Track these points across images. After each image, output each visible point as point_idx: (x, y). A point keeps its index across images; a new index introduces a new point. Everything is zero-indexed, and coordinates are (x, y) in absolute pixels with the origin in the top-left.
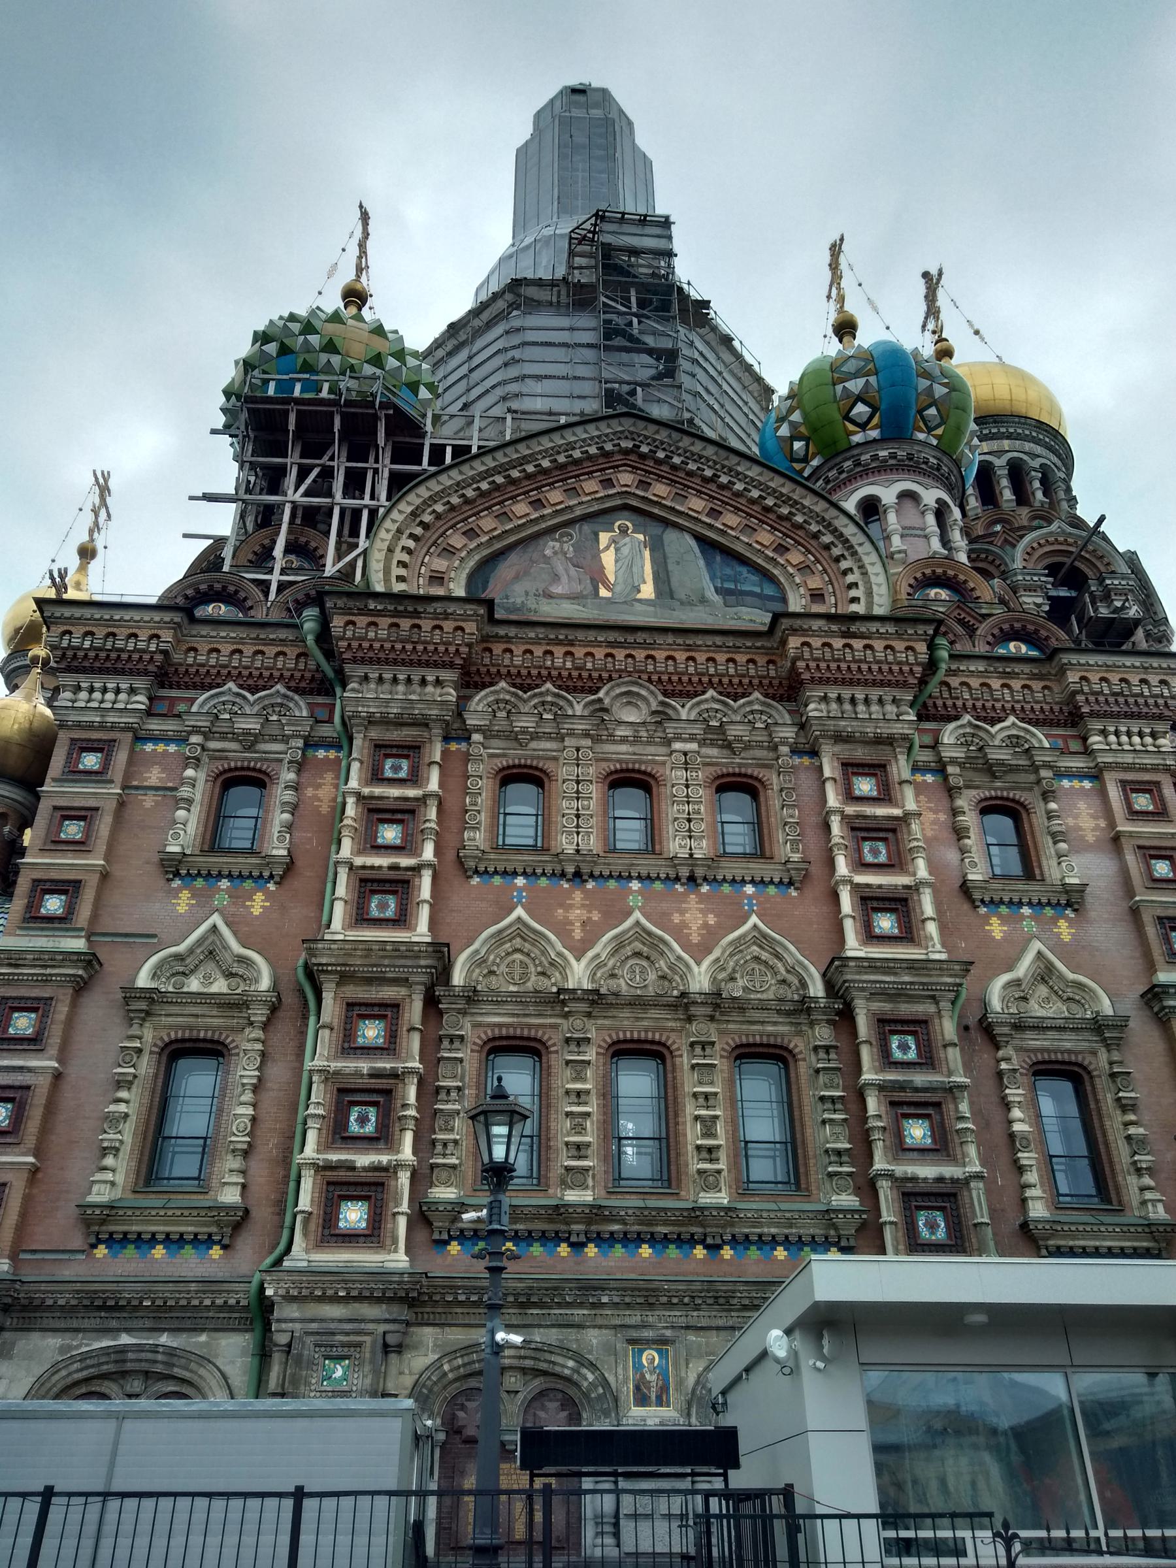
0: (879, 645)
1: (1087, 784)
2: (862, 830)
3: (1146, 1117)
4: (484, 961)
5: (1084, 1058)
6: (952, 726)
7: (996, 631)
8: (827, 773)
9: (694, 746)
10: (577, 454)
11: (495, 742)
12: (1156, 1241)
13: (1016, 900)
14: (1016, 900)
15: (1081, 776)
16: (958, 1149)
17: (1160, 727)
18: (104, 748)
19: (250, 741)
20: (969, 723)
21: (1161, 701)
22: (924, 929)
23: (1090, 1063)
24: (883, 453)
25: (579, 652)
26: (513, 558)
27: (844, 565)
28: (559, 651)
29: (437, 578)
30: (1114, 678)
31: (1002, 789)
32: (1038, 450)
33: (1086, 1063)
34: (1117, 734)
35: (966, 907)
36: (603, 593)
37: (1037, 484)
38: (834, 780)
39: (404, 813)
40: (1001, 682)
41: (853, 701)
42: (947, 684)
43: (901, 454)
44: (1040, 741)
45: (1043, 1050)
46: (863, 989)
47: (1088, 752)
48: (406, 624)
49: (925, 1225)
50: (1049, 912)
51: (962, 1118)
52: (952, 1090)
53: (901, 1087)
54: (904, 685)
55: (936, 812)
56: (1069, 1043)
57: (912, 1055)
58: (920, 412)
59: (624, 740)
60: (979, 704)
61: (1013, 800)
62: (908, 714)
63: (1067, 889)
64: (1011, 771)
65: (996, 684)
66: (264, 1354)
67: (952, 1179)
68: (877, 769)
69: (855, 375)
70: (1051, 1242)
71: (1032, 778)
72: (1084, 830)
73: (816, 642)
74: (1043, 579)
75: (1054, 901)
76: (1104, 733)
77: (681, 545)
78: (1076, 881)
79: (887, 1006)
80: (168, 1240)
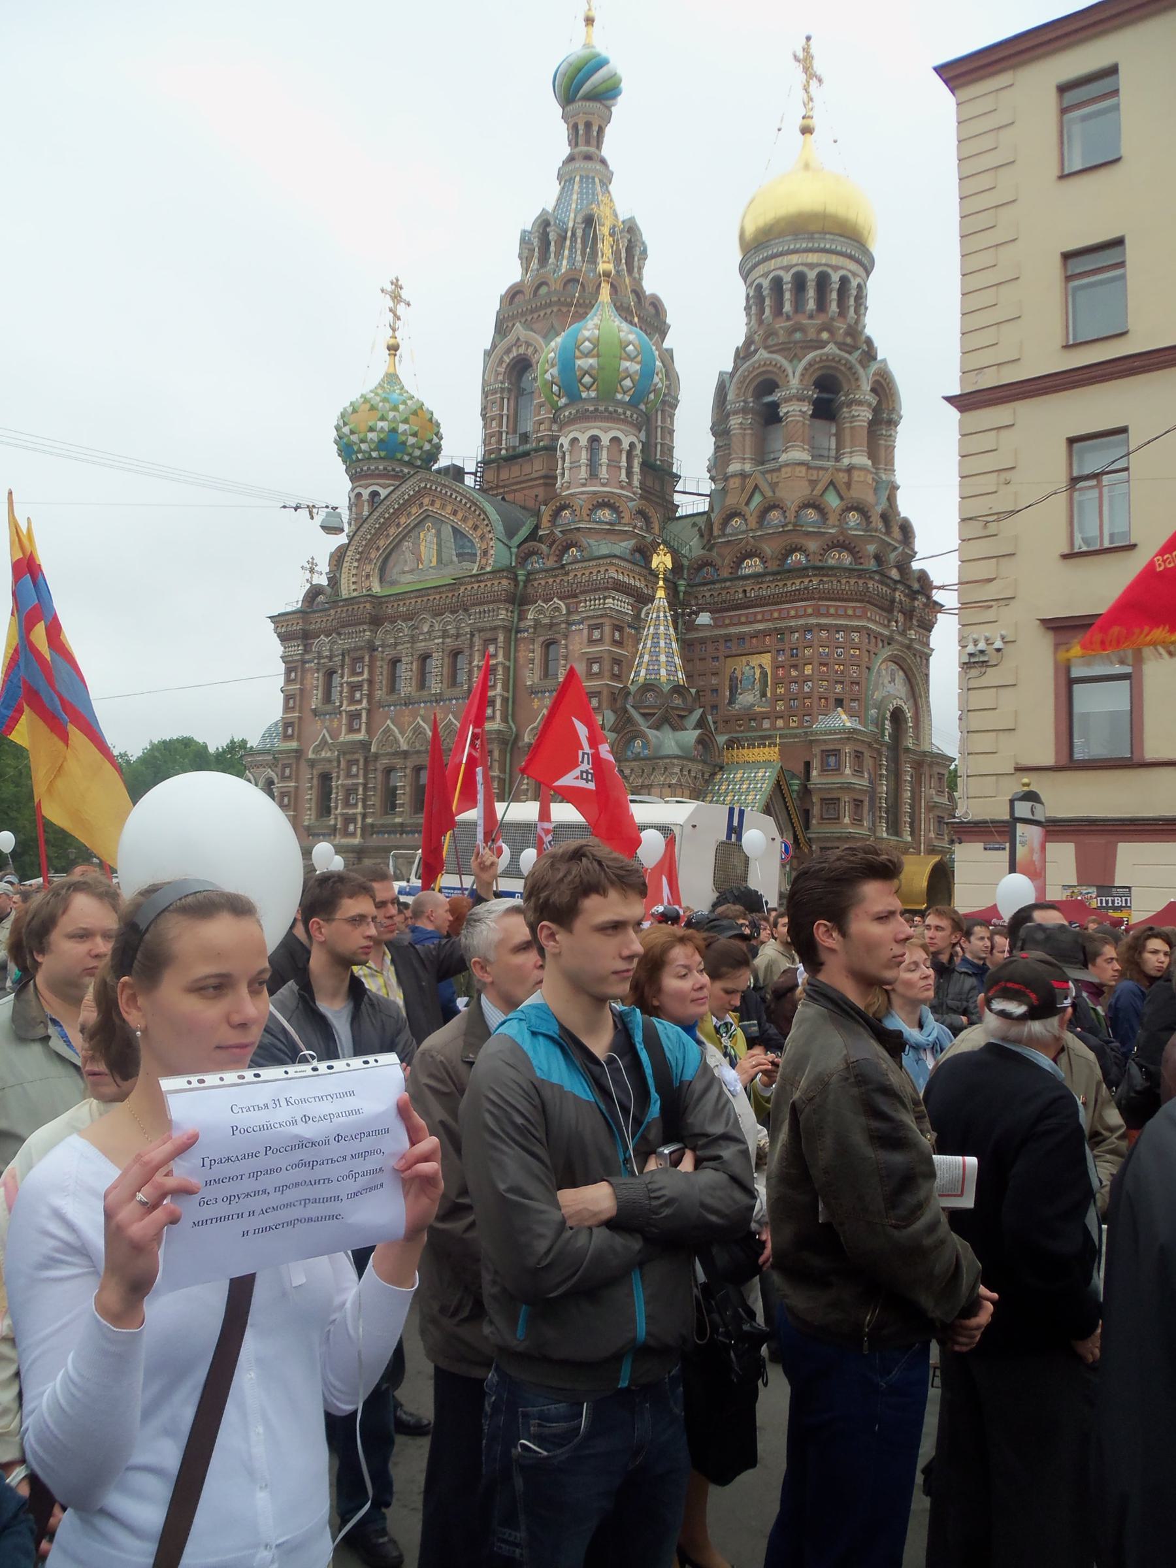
1: (581, 627)
4: (381, 741)
7: (560, 548)
9: (440, 640)
10: (406, 497)
11: (387, 649)
24: (567, 413)
25: (407, 602)
26: (394, 555)
28: (401, 603)
32: (794, 259)
36: (420, 567)
40: (552, 580)
41: (485, 611)
43: (574, 412)
48: (350, 608)
54: (500, 601)
58: (580, 381)
59: (422, 641)
68: (494, 640)
74: (742, 404)
76: (586, 600)
77: (447, 531)
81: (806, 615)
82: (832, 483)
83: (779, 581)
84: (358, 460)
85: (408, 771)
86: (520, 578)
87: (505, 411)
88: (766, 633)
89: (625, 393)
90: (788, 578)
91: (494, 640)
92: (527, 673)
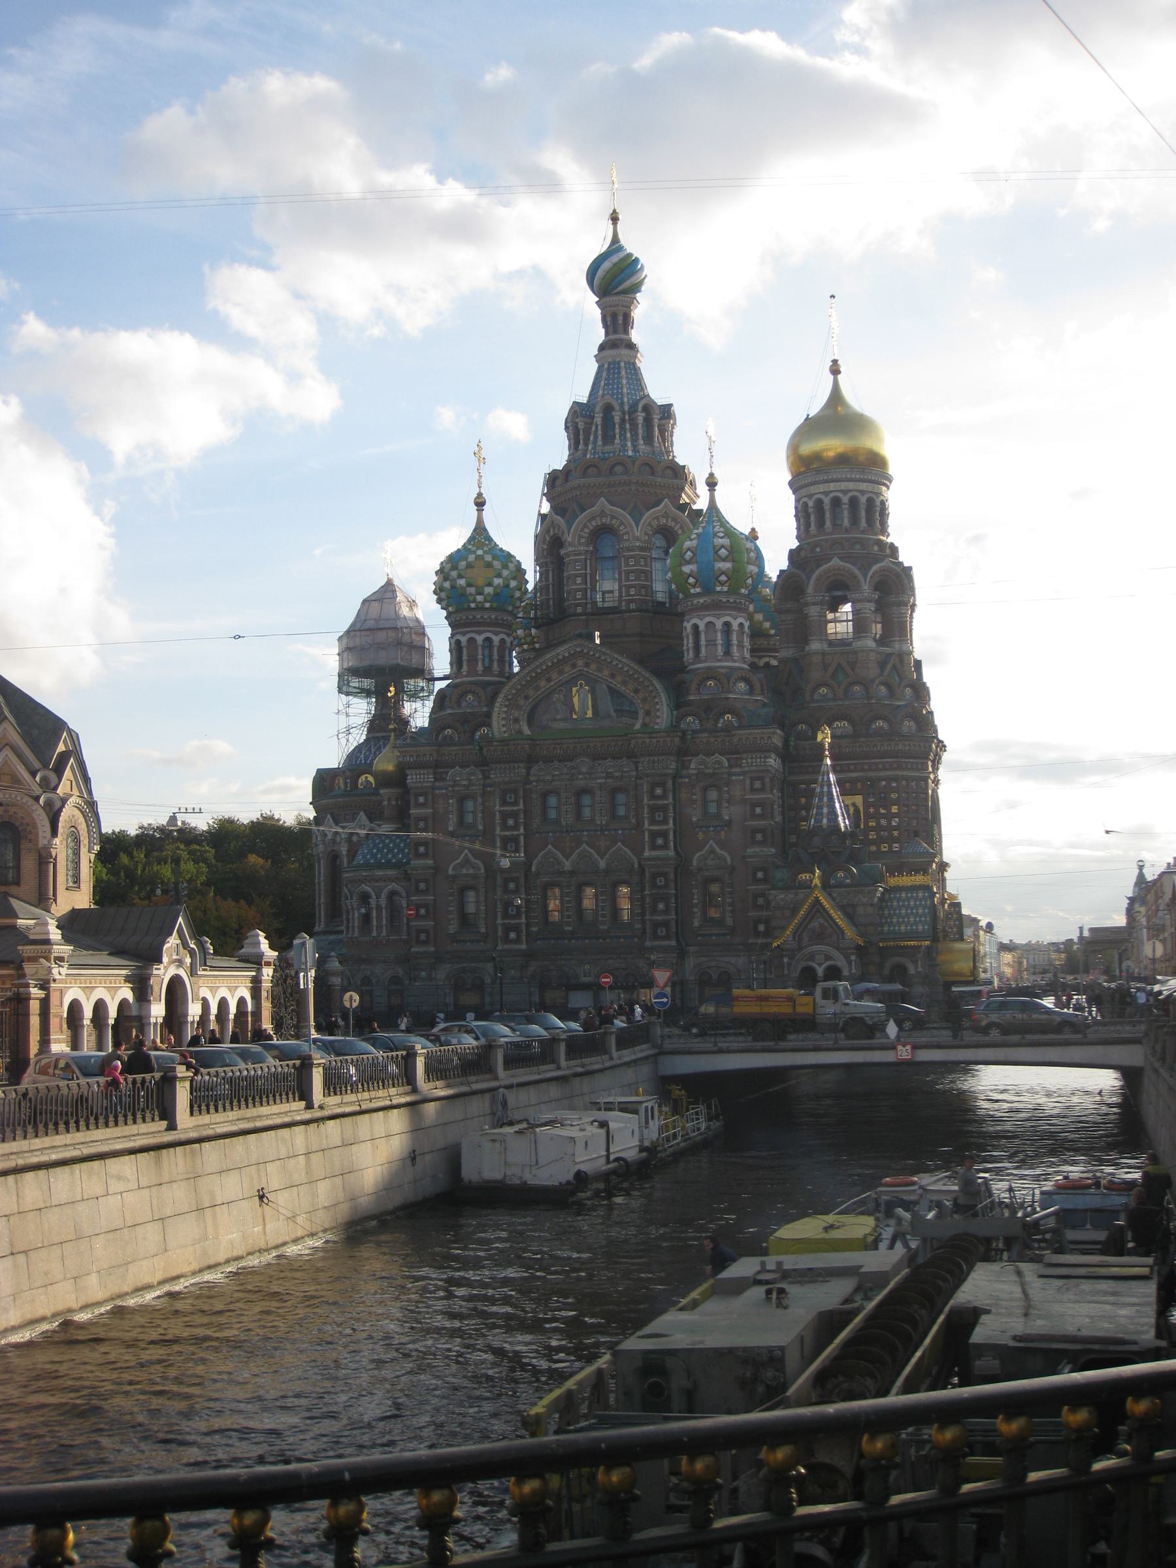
0: (661, 740)
1: (741, 777)
2: (653, 809)
17: (767, 754)
18: (424, 794)
19: (467, 787)
24: (701, 601)
27: (656, 700)
29: (516, 720)
32: (851, 485)
34: (752, 758)
36: (575, 716)
37: (846, 513)
39: (515, 815)
47: (740, 766)
58: (717, 579)
65: (712, 740)
66: (495, 967)
68: (663, 785)
69: (689, 562)
73: (640, 741)
78: (727, 818)
80: (469, 941)
82: (894, 666)
84: (470, 609)
85: (573, 888)
87: (588, 571)
88: (857, 780)
89: (747, 588)
91: (663, 785)
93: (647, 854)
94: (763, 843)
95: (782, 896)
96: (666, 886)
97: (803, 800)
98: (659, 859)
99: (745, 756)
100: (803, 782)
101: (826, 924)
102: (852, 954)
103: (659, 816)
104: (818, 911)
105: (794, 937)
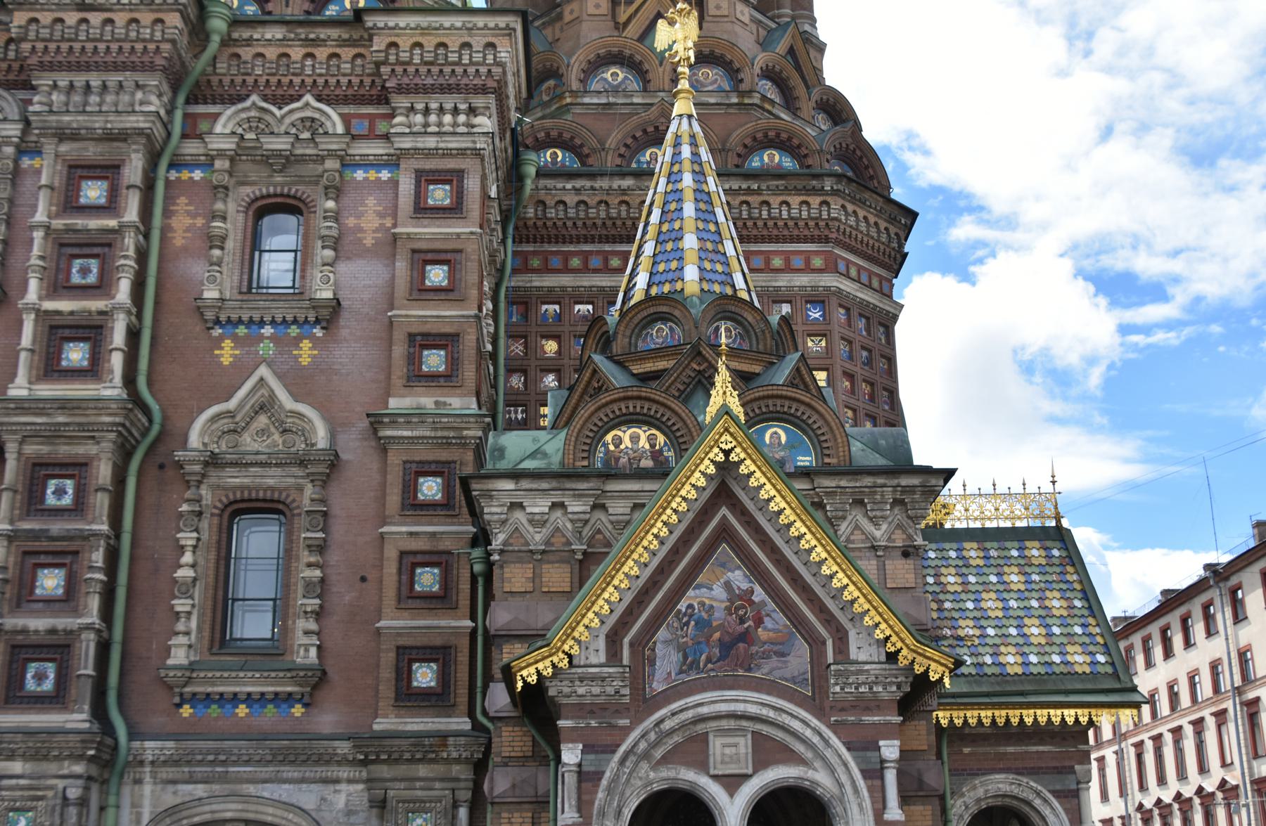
1: (385, 175)
3: (334, 557)
5: (288, 496)
6: (233, 109)
8: (44, 181)
12: (300, 685)
13: (256, 317)
14: (256, 317)
15: (378, 165)
16: (82, 600)
17: (479, 101)
20: (254, 104)
21: (483, 70)
22: (109, 361)
23: (294, 501)
30: (429, 43)
31: (283, 185)
33: (288, 501)
34: (427, 111)
35: (199, 328)
38: (51, 188)
40: (303, 51)
41: (88, 87)
42: (238, 56)
44: (334, 125)
45: (242, 488)
46: (14, 432)
49: (33, 677)
50: (294, 331)
51: (91, 568)
52: (87, 537)
53: (35, 535)
54: (149, 68)
55: (194, 216)
56: (272, 479)
57: (67, 500)
60: (274, 80)
61: (294, 197)
62: (150, 103)
63: (316, 305)
64: (297, 161)
65: (297, 53)
67: (65, 630)
68: (109, 171)
70: (187, 689)
71: (320, 168)
72: (365, 232)
75: (301, 319)
78: (329, 295)
79: (45, 449)
81: (808, 269)
82: (791, 51)
83: (749, 191)
86: (218, 25)
90: (776, 191)
91: (109, 171)
92: (197, 269)
93: (19, 389)
94: (447, 379)
95: (539, 506)
96: (79, 508)
97: (551, 347)
98: (64, 405)
99: (401, 102)
100: (550, 296)
101: (759, 594)
102: (888, 731)
103: (84, 271)
104: (724, 533)
105: (613, 654)
